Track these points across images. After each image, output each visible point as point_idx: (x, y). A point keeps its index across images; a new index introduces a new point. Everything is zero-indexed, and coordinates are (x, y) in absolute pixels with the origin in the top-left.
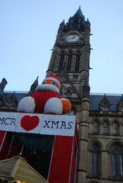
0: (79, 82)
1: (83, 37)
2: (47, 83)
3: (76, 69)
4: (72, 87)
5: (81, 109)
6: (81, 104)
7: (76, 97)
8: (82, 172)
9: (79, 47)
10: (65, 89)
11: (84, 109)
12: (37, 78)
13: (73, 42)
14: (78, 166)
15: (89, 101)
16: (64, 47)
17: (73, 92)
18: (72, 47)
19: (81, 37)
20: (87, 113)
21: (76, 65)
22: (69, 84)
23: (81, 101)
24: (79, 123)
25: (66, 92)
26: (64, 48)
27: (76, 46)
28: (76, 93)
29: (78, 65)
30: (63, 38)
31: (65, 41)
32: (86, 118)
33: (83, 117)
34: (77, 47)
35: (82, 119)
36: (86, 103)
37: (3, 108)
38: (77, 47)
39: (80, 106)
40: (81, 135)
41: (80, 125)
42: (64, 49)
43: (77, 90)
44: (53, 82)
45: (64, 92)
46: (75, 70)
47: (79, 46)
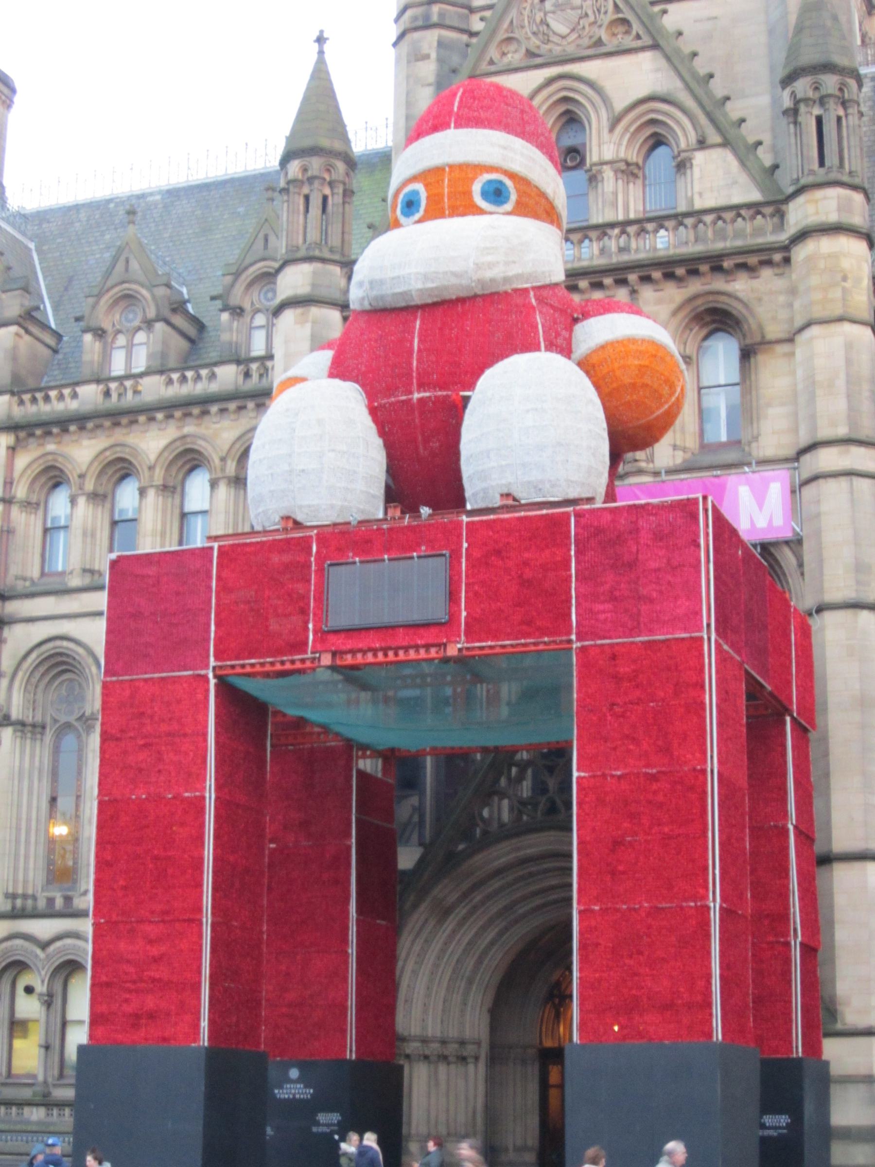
2: (435, 211)
4: (679, 84)
5: (799, 322)
6: (787, 260)
7: (737, 198)
8: (857, 866)
10: (612, 129)
11: (818, 312)
12: (321, 52)
14: (806, 836)
15: (858, 219)
17: (702, 144)
20: (849, 346)
23: (781, 225)
24: (791, 452)
25: (633, 156)
28: (726, 144)
32: (849, 396)
33: (819, 392)
35: (814, 428)
36: (825, 245)
37: (73, 405)
39: (780, 283)
40: (821, 561)
41: (805, 475)
43: (734, 110)
44: (487, 177)
45: (609, 153)
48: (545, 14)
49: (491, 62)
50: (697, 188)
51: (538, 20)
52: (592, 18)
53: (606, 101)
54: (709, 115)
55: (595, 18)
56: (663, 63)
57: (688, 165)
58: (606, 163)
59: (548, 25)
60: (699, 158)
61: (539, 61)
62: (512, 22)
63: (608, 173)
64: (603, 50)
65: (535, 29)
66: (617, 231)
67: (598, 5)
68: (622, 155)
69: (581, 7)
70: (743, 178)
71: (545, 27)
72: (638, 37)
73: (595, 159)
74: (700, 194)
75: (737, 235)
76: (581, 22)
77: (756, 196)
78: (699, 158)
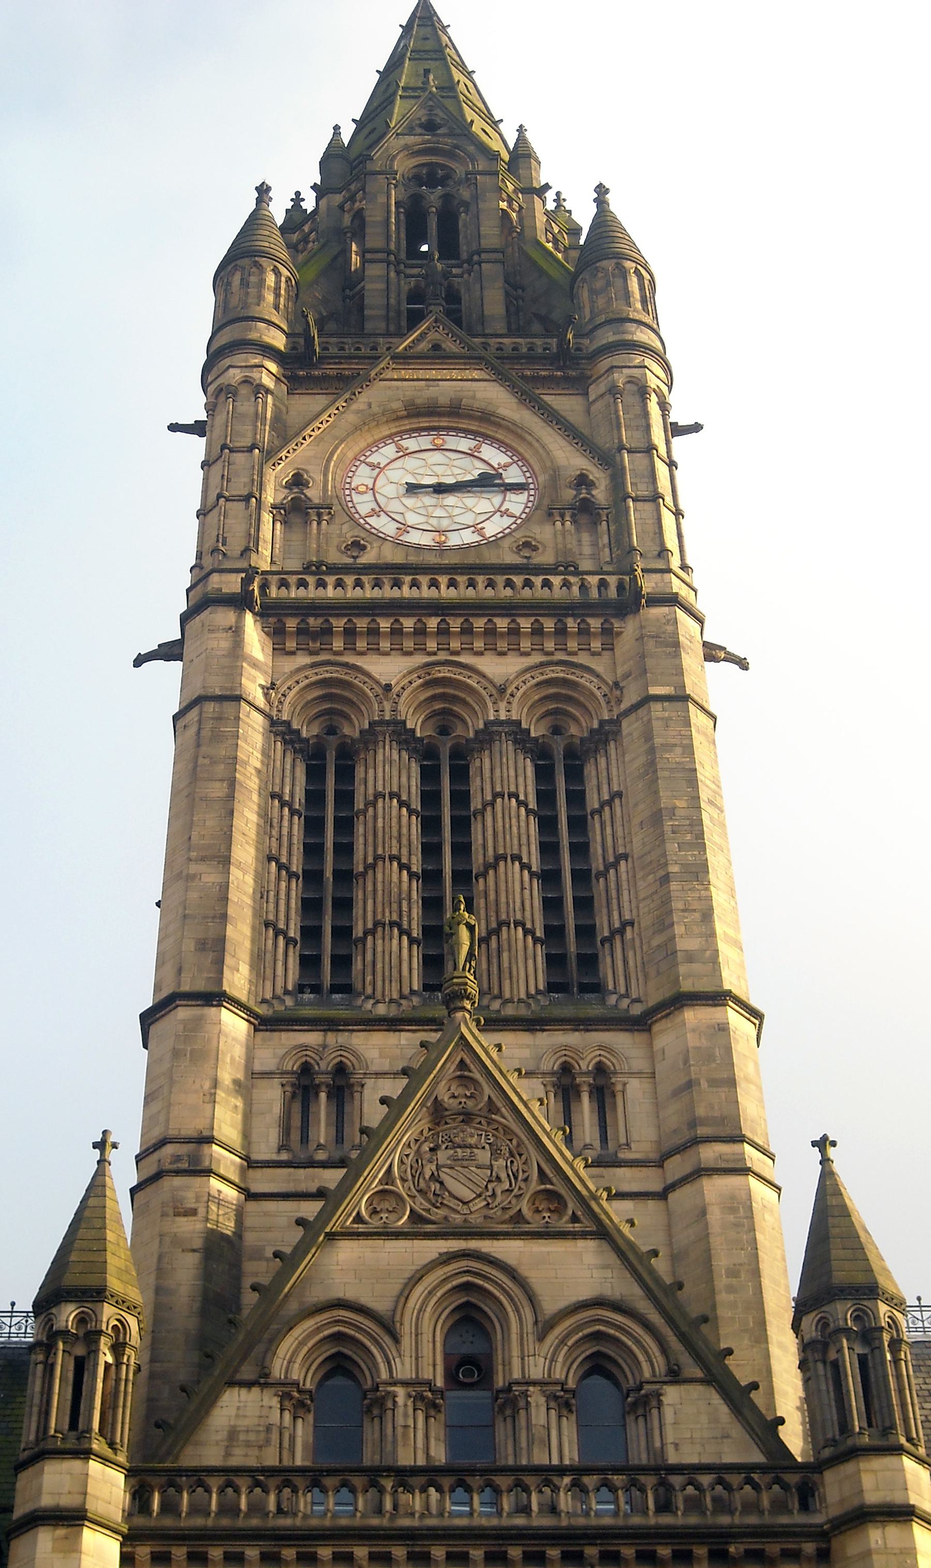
0: (649, 1180)
1: (582, 481)
3: (555, 962)
4: (637, 1291)
7: (729, 1458)
9: (561, 631)
13: (454, 540)
16: (339, 624)
17: (675, 1376)
18: (455, 624)
19: (555, 474)
21: (552, 905)
22: (588, 1250)
26: (350, 633)
27: (509, 609)
29: (584, 904)
30: (298, 481)
31: (343, 532)
34: (525, 624)
38: (537, 631)
42: (350, 647)
45: (537, 1371)
46: (552, 987)
47: (560, 610)
48: (438, 1168)
49: (359, 1219)
50: (670, 1437)
51: (428, 1174)
52: (507, 1186)
53: (532, 1299)
54: (683, 1338)
55: (511, 1185)
56: (612, 1258)
57: (654, 1403)
58: (534, 1383)
59: (441, 1183)
60: (672, 1394)
61: (430, 1228)
62: (390, 1170)
63: (537, 1398)
64: (526, 1228)
65: (422, 1185)
66: (567, 1480)
67: (515, 1169)
68: (558, 1374)
69: (491, 1167)
70: (737, 1431)
71: (438, 1185)
72: (575, 1219)
73: (516, 1375)
74: (676, 1445)
75: (751, 1507)
76: (490, 1186)
77: (757, 1457)
78: (672, 1394)
